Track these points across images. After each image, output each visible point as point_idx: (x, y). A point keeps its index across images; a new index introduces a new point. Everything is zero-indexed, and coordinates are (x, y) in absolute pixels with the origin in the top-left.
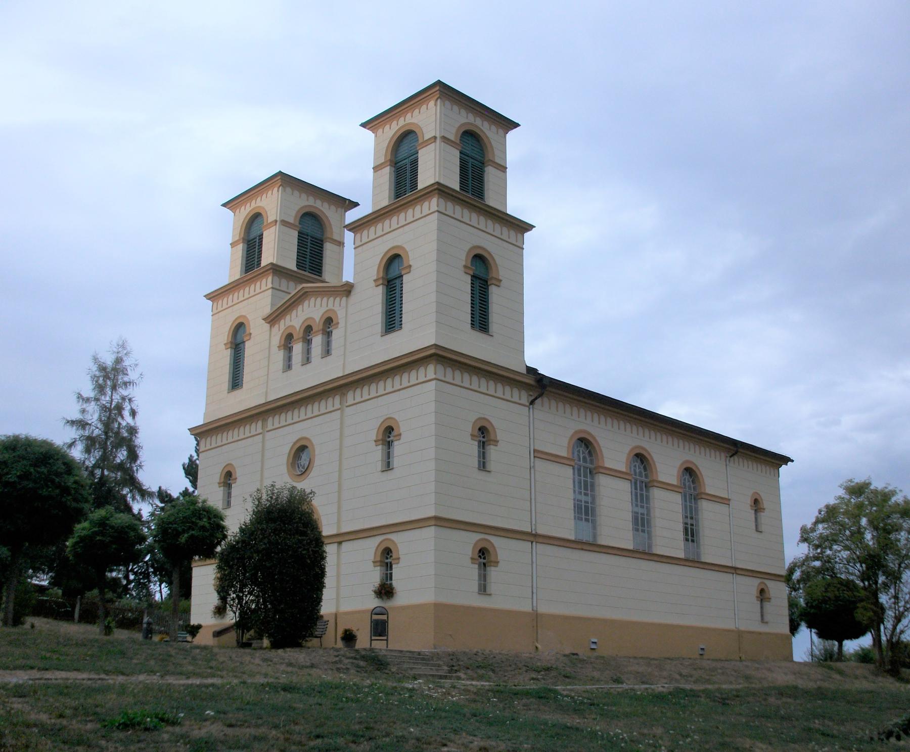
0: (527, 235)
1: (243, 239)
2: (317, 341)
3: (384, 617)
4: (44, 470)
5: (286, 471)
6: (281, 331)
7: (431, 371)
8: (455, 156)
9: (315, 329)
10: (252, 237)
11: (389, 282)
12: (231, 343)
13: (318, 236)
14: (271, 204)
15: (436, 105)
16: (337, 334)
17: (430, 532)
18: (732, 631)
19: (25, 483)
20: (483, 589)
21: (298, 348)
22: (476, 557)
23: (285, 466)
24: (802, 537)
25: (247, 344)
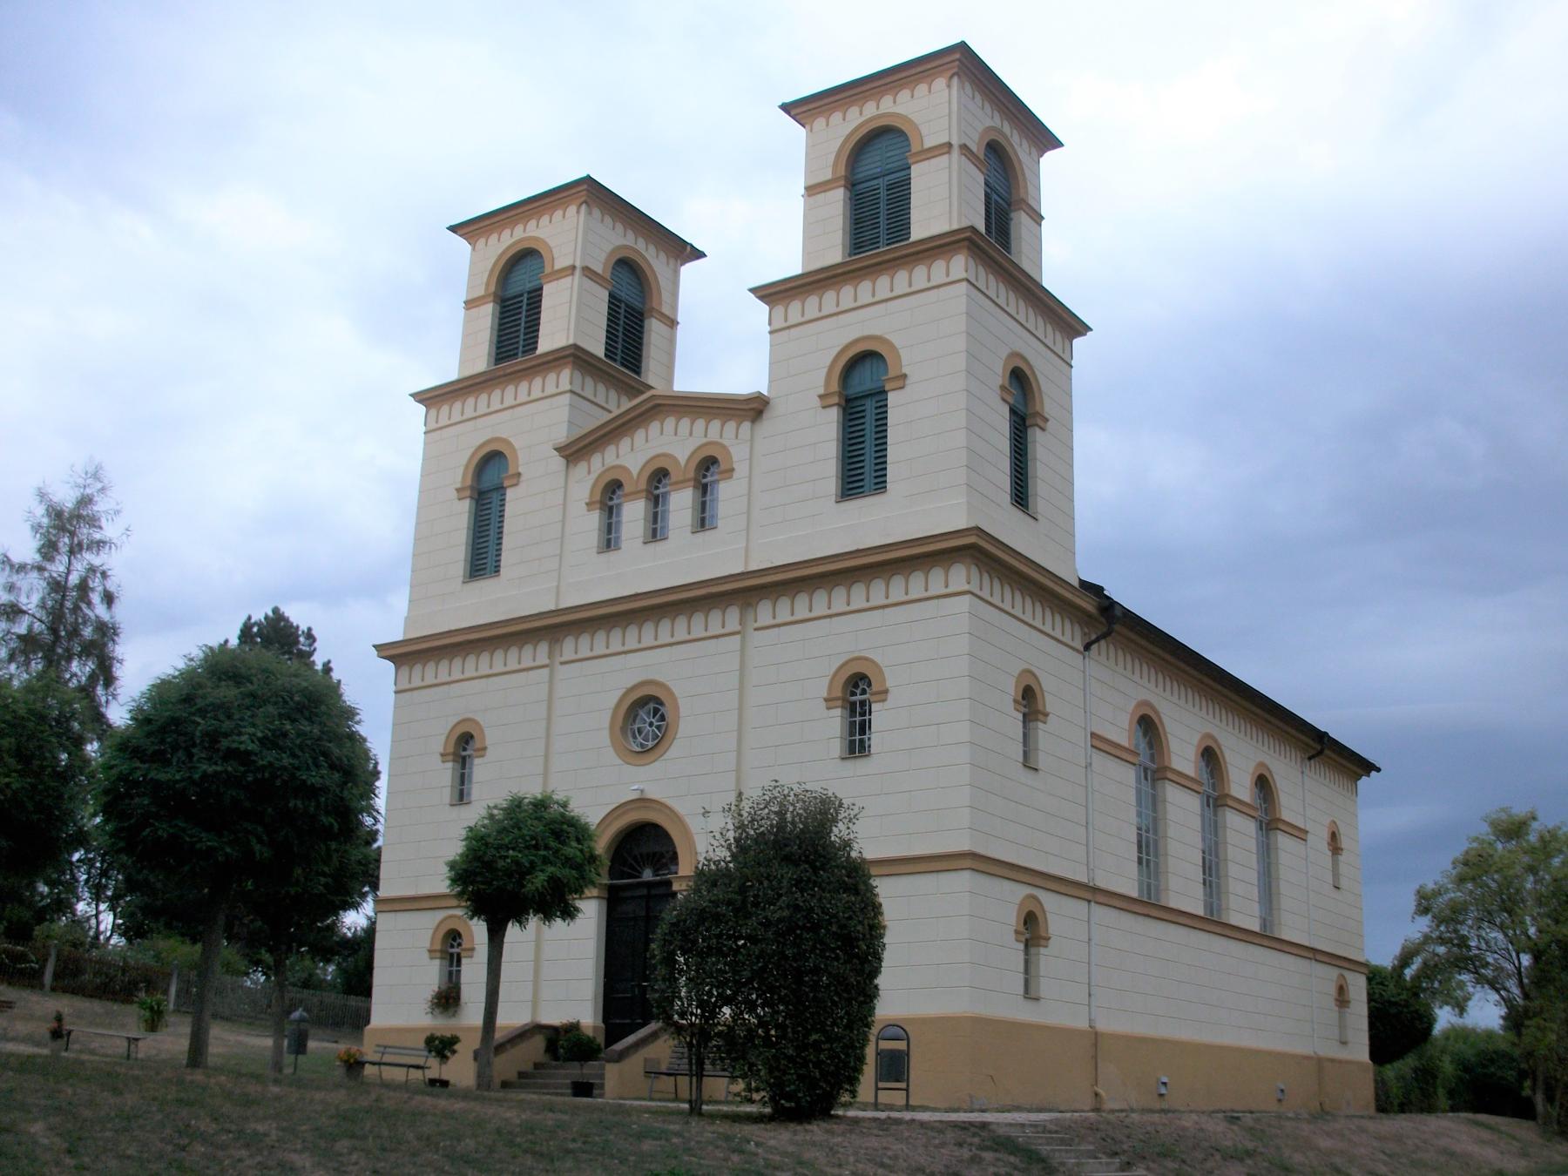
0: (1077, 342)
1: (495, 295)
2: (681, 502)
3: (901, 1045)
4: (305, 727)
5: (608, 741)
6: (594, 475)
7: (960, 576)
8: (976, 182)
9: (675, 476)
10: (513, 290)
11: (848, 400)
12: (472, 488)
13: (637, 304)
14: (567, 239)
15: (949, 86)
16: (727, 493)
17: (961, 881)
18: (1307, 1058)
19: (270, 756)
20: (1029, 993)
21: (634, 513)
22: (1022, 928)
23: (606, 733)
24: (1419, 904)
25: (510, 494)
